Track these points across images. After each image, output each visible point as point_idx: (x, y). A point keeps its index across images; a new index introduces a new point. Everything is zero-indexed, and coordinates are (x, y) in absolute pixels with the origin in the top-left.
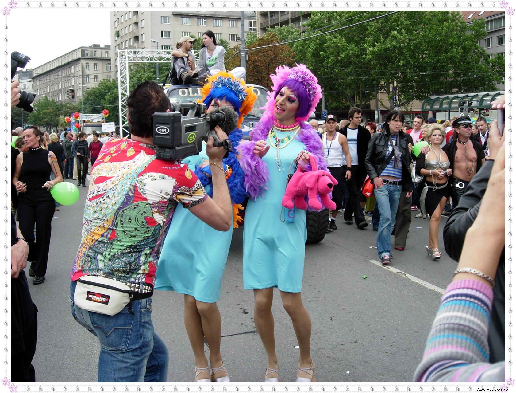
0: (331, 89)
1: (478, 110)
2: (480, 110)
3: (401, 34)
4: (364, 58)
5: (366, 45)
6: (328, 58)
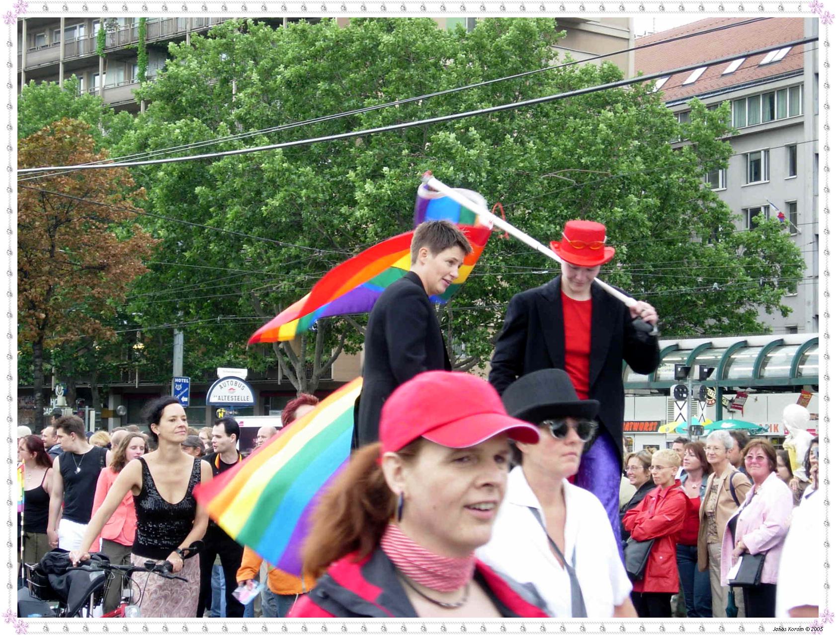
0: (217, 308)
1: (713, 394)
2: (722, 391)
3: (469, 143)
4: (346, 218)
5: (351, 174)
6: (222, 207)
